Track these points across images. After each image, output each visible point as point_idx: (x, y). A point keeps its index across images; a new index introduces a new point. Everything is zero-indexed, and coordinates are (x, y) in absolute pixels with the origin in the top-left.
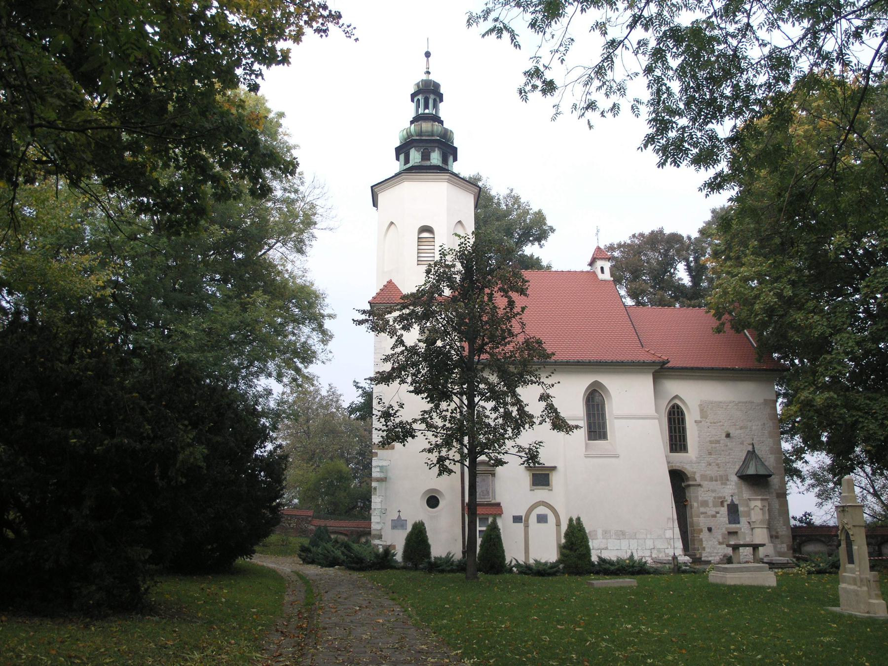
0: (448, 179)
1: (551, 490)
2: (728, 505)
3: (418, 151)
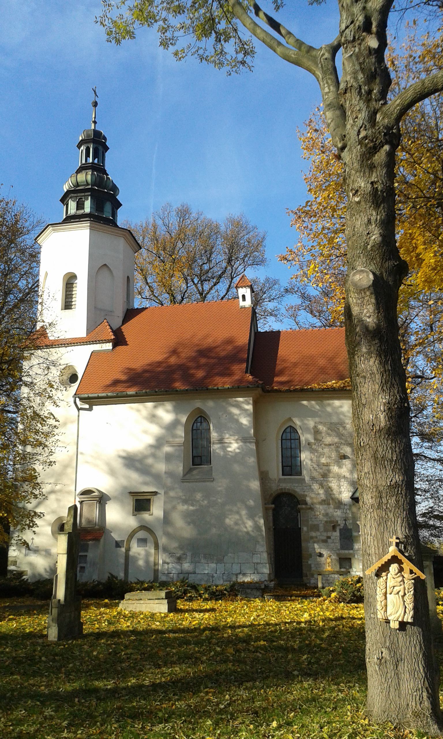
0: (54, 230)
2: (340, 530)
3: (74, 201)
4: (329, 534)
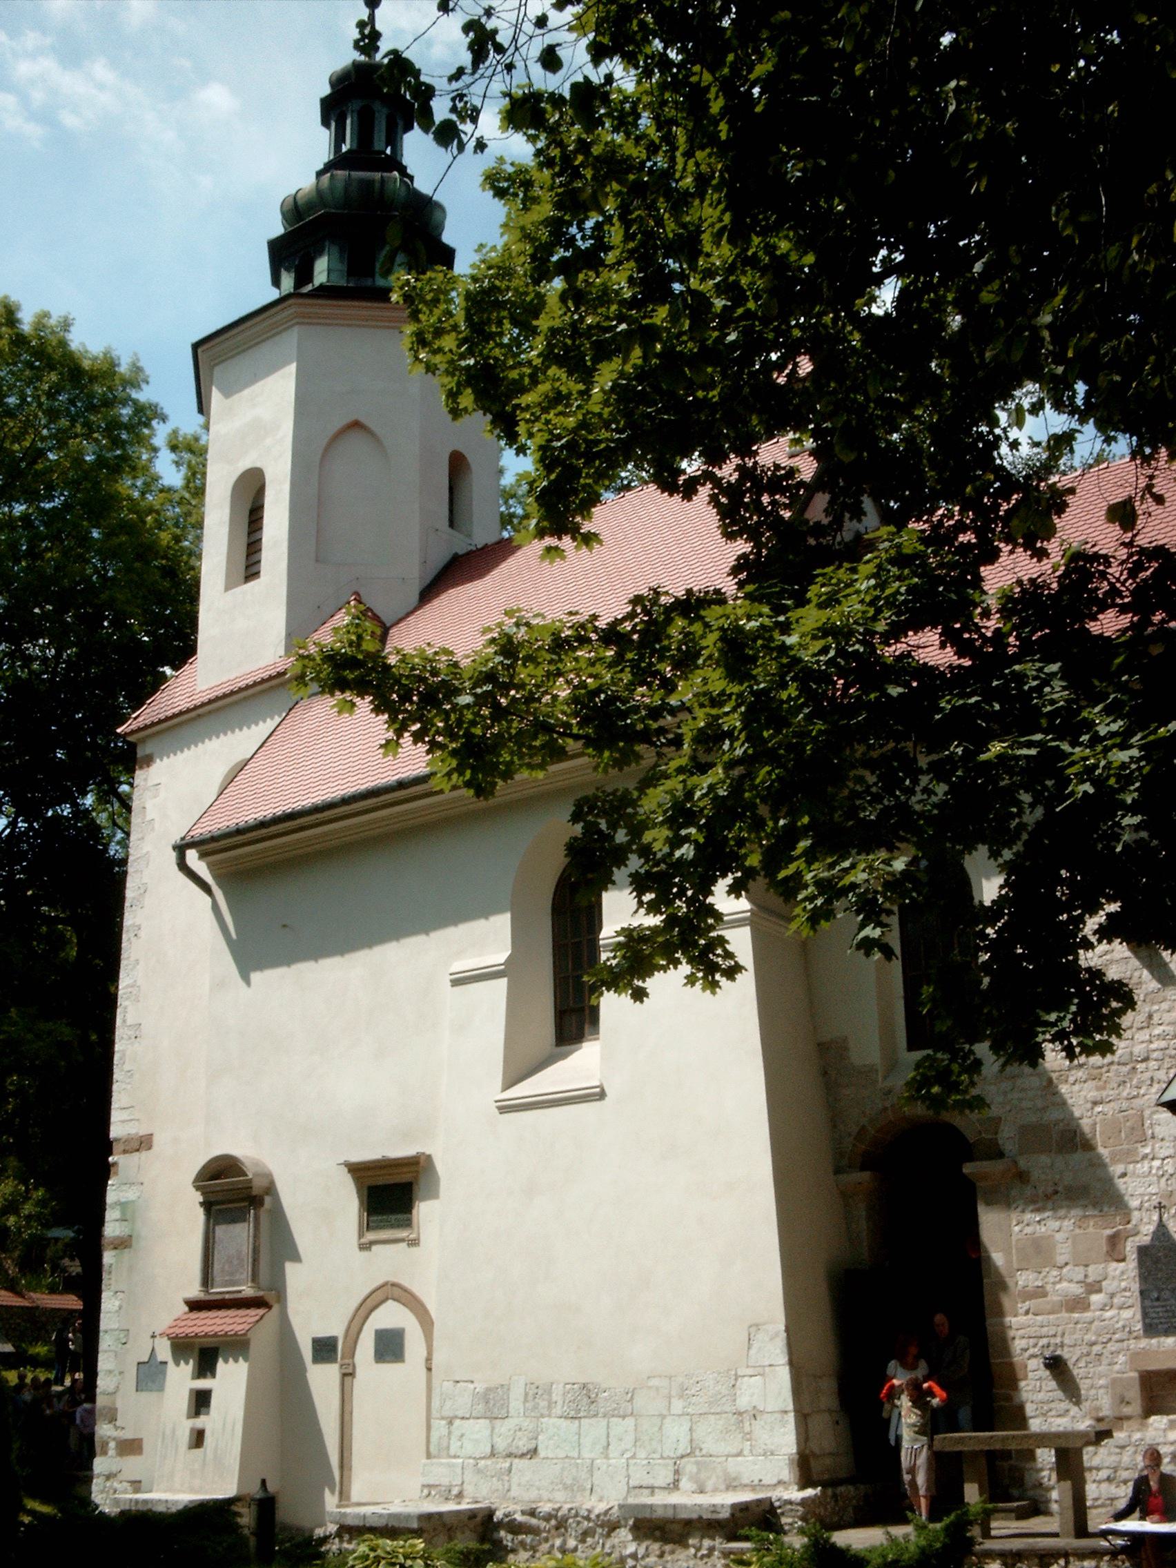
1: (414, 1243)
2: (1143, 1251)
4: (1094, 1272)
